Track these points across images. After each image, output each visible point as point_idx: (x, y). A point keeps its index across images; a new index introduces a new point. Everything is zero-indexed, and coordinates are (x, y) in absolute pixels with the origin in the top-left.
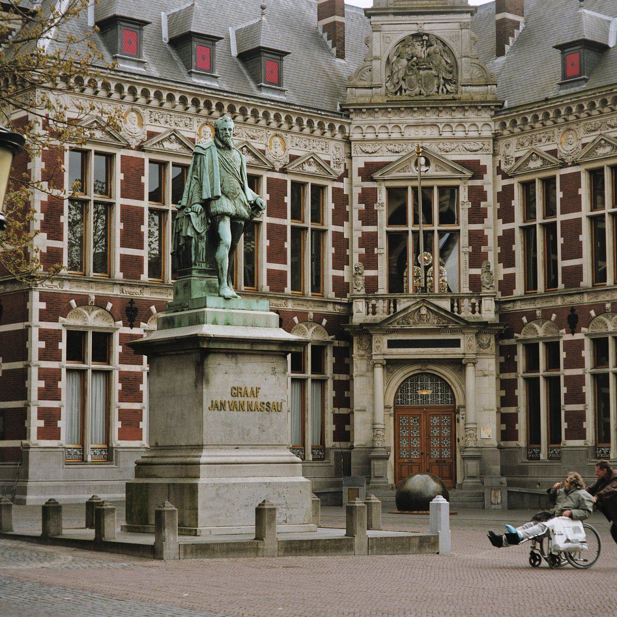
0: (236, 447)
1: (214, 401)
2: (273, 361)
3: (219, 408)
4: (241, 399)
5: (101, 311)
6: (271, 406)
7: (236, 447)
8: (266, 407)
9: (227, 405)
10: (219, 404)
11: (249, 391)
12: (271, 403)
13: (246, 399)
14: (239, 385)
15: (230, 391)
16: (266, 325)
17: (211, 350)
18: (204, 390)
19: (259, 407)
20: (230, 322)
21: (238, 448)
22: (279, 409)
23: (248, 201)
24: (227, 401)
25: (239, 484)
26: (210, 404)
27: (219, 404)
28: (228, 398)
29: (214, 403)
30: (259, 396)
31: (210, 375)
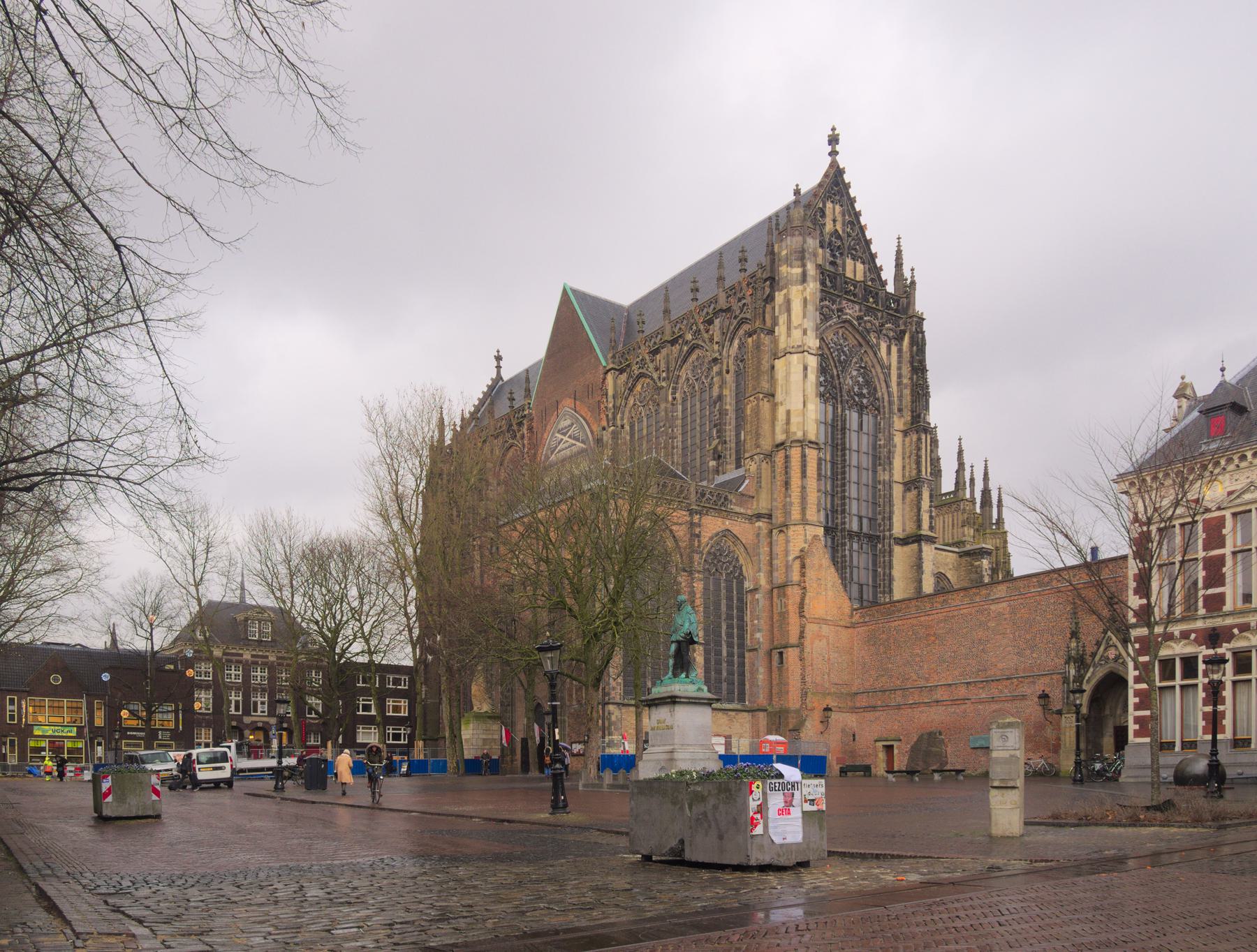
5: (1186, 641)
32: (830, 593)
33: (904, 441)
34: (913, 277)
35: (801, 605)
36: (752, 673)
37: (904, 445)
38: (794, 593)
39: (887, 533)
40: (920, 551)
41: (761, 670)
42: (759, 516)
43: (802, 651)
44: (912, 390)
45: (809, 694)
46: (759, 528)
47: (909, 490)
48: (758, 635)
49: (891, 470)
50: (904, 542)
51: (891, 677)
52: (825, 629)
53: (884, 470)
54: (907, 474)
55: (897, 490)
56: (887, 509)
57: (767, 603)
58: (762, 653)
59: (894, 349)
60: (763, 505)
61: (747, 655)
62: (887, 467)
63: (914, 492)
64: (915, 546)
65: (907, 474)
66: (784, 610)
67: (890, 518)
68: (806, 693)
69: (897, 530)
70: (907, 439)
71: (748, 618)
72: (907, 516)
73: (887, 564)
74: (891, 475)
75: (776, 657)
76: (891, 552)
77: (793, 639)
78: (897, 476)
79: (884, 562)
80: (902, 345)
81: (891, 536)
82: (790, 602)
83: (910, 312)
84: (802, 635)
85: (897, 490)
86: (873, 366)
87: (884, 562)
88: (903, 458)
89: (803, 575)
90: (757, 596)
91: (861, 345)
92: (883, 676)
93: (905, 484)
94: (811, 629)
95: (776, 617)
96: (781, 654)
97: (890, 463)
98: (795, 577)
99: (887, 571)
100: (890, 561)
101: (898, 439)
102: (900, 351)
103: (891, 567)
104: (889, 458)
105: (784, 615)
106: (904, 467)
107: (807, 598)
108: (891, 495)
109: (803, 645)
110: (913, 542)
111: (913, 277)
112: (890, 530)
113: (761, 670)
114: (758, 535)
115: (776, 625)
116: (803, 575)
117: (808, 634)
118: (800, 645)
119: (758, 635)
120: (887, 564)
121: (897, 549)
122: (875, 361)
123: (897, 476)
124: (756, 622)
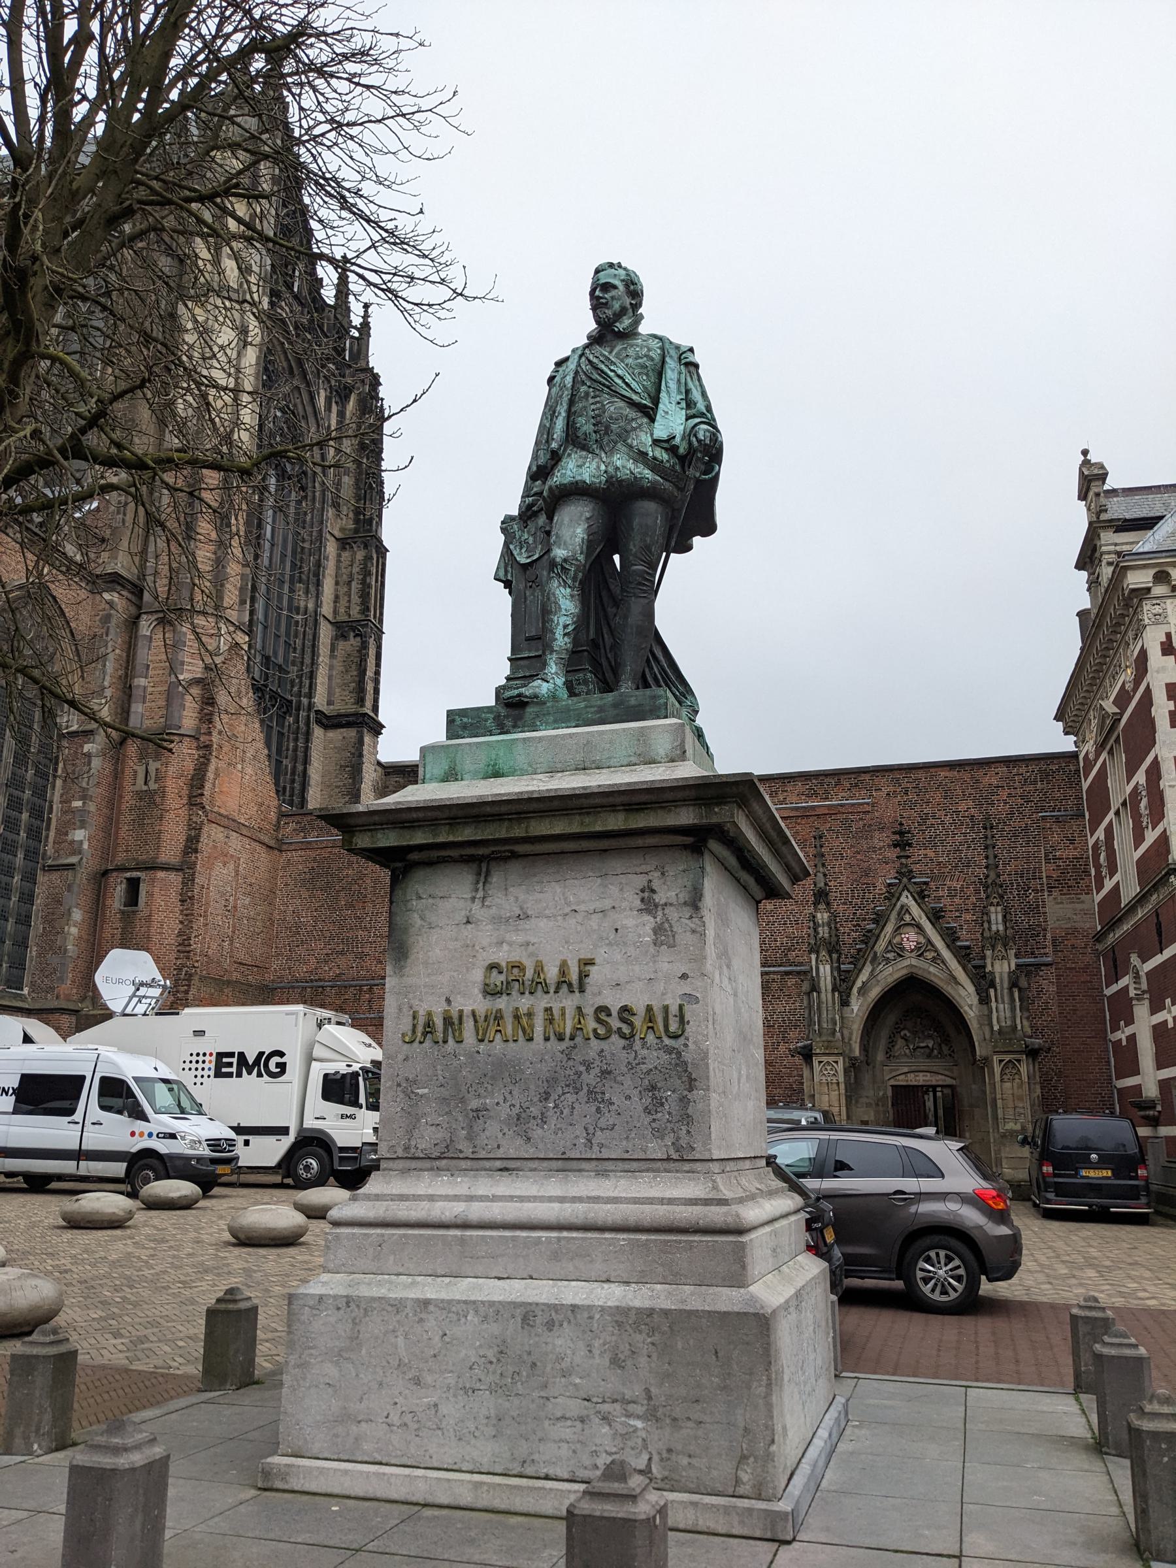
0: (498, 1164)
1: (422, 1012)
2: (644, 868)
3: (440, 1035)
4: (524, 1003)
6: (638, 1021)
7: (498, 1164)
8: (615, 1023)
9: (469, 1024)
10: (439, 1022)
11: (552, 973)
12: (640, 1010)
13: (541, 1002)
14: (517, 955)
15: (478, 975)
16: (634, 759)
17: (414, 856)
18: (390, 982)
19: (591, 1024)
20: (505, 768)
21: (506, 1169)
22: (673, 1027)
23: (656, 442)
24: (467, 1010)
25: (445, 1305)
26: (406, 1025)
27: (439, 1022)
28: (473, 1002)
29: (421, 1021)
30: (589, 989)
31: (412, 930)
32: (249, 770)
33: (339, 556)
34: (366, 316)
35: (197, 781)
36: (49, 920)
37: (339, 561)
38: (184, 755)
39: (305, 701)
40: (361, 742)
41: (77, 915)
42: (115, 580)
43: (189, 881)
44: (357, 481)
45: (195, 981)
46: (110, 604)
47: (344, 637)
48: (79, 835)
49: (318, 596)
50: (330, 722)
51: (362, 956)
52: (236, 843)
53: (307, 592)
54: (342, 610)
55: (325, 633)
56: (308, 661)
57: (109, 768)
58: (82, 877)
59: (334, 408)
60: (121, 563)
61: (41, 878)
62: (312, 588)
63: (354, 642)
64: (351, 733)
65: (342, 610)
66: (153, 786)
67: (312, 676)
68: (189, 977)
69: (320, 700)
70: (346, 555)
71: (56, 794)
72: (337, 681)
73: (300, 754)
74: (318, 605)
75: (118, 892)
76: (308, 735)
77: (170, 851)
78: (327, 609)
79: (295, 750)
80: (344, 407)
81: (310, 706)
82: (172, 770)
83: (362, 364)
84: (192, 845)
85: (325, 633)
86: (305, 417)
87: (295, 750)
88: (337, 583)
89: (206, 718)
90: (87, 748)
91: (291, 372)
92: (342, 953)
93: (337, 625)
94: (212, 835)
95: (128, 801)
96: (133, 886)
97: (318, 584)
98: (188, 719)
99: (300, 768)
100: (307, 749)
101: (331, 548)
102: (341, 414)
103: (306, 761)
104: (317, 575)
105: (150, 800)
106: (337, 597)
107: (212, 768)
108: (315, 637)
109: (192, 866)
110: (348, 725)
111: (366, 316)
112: (310, 695)
113: (77, 915)
114: (107, 619)
115: (126, 818)
116: (206, 718)
117: (205, 843)
118: (186, 867)
119: (79, 835)
120: (300, 754)
121: (318, 732)
122: (309, 409)
123: (327, 609)
124: (78, 804)
